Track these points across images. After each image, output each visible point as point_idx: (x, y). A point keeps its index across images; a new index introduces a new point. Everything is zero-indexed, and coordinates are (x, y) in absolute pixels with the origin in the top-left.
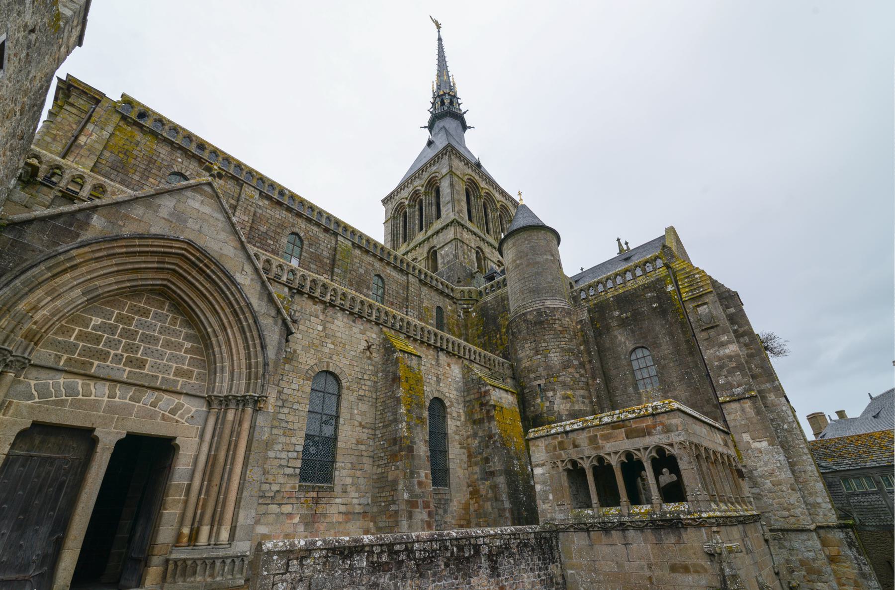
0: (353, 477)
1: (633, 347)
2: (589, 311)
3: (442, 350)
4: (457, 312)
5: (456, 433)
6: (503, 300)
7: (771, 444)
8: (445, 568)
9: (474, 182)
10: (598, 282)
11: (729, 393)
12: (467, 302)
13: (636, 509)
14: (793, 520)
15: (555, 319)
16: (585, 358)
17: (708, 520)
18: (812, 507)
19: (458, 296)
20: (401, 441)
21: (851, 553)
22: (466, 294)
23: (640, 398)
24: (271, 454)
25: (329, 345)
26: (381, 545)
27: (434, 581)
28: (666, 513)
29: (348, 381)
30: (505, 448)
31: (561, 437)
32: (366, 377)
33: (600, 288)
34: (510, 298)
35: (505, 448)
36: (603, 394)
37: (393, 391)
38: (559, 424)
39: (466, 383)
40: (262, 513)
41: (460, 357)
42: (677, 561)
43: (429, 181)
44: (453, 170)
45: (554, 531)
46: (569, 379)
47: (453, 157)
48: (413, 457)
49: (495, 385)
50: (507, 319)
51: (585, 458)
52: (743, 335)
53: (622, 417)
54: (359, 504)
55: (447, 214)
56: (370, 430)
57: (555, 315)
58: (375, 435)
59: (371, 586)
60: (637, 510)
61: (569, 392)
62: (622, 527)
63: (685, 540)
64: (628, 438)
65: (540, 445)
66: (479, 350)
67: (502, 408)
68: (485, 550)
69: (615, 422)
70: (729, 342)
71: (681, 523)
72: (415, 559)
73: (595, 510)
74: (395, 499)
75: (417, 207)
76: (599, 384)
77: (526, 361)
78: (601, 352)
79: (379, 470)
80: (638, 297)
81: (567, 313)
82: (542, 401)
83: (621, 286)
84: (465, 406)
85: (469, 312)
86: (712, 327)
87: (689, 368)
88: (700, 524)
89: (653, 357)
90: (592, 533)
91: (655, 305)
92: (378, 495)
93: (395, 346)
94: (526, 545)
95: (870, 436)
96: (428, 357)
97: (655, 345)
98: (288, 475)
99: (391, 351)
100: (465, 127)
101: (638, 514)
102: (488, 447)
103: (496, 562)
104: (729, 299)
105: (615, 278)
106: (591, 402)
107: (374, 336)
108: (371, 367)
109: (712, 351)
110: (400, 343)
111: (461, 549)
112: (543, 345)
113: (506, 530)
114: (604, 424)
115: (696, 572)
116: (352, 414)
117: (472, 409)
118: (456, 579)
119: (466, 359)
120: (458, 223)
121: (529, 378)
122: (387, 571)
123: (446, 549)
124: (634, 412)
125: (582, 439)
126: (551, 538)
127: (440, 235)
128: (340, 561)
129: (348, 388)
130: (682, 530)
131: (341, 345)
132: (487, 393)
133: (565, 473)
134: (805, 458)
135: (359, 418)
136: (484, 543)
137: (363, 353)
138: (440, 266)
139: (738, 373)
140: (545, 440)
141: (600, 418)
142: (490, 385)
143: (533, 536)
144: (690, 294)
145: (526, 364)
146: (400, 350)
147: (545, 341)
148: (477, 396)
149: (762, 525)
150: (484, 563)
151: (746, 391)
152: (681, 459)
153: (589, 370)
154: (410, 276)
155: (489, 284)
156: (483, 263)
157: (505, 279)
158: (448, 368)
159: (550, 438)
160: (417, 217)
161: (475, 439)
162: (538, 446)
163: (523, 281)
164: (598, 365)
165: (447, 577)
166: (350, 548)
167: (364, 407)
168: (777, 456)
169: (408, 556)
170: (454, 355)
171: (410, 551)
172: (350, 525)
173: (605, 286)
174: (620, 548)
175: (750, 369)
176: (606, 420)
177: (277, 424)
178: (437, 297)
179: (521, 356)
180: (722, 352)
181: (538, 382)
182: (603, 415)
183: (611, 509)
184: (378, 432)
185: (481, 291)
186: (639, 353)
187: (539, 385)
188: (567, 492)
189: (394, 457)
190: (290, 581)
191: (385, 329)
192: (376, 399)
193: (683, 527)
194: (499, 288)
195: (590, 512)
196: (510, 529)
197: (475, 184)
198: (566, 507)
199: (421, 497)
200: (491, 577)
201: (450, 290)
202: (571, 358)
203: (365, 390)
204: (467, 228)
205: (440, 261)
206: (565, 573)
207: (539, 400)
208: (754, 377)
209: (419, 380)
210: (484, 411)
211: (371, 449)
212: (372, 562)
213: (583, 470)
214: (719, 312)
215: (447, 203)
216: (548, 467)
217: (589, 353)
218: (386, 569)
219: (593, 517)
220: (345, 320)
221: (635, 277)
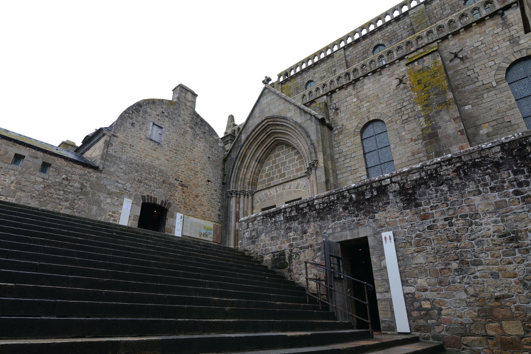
29: (390, 117)
59: (286, 229)
72: (315, 210)
118: (357, 216)
123: (344, 197)
129: (391, 121)
131: (375, 98)
135: (409, 136)
165: (347, 216)
169: (310, 209)
177: (345, 170)
203: (408, 114)
212: (286, 217)
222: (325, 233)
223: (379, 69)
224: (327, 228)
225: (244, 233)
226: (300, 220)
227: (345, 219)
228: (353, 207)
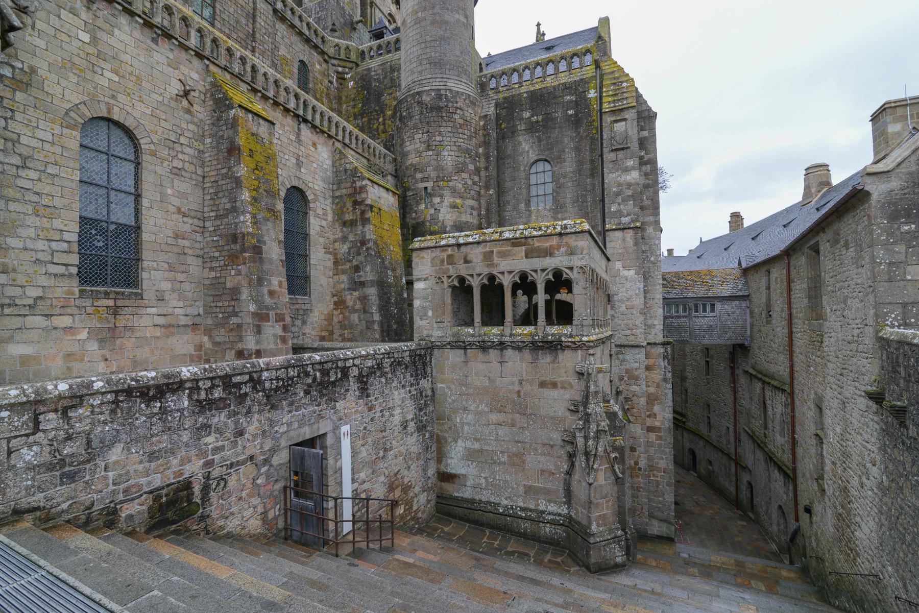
0: (173, 281)
1: (536, 158)
2: (497, 106)
3: (305, 121)
4: (328, 75)
6: (392, 70)
7: (637, 273)
8: (305, 396)
10: (514, 70)
11: (616, 221)
12: (344, 64)
13: (519, 330)
14: (632, 338)
15: (457, 108)
16: (482, 164)
17: (587, 344)
18: (649, 327)
19: (331, 51)
20: (244, 239)
21: (662, 363)
22: (342, 52)
23: (530, 216)
24: (13, 242)
25: (107, 74)
26: (212, 379)
27: (290, 412)
28: (548, 335)
29: (152, 142)
30: (380, 257)
32: (182, 140)
33: (515, 78)
34: (403, 67)
35: (380, 257)
36: (494, 207)
37: (230, 168)
38: (451, 235)
39: (336, 173)
40: (14, 327)
41: (330, 137)
42: (548, 378)
45: (429, 348)
46: (460, 186)
48: (261, 260)
49: (374, 180)
50: (395, 98)
51: (475, 276)
52: (646, 163)
53: (526, 233)
54: (186, 315)
56: (196, 221)
57: (457, 102)
58: (204, 227)
59: (198, 429)
60: (520, 331)
61: (458, 201)
62: (502, 346)
63: (560, 361)
64: (527, 257)
65: (426, 257)
66: (356, 131)
67: (380, 210)
68: (355, 372)
69: (516, 238)
70: (633, 168)
71: (561, 345)
72: (264, 390)
73: (477, 329)
74: (237, 310)
76: (491, 195)
77: (413, 156)
78: (500, 158)
79: (213, 274)
80: (555, 97)
82: (426, 207)
83: (539, 80)
84: (333, 203)
85: (344, 79)
86: (623, 149)
87: (586, 190)
88: (578, 346)
89: (553, 173)
90: (469, 351)
91: (570, 112)
92: (212, 304)
93: (231, 98)
94: (399, 364)
95: (699, 273)
96: (285, 127)
97: (560, 160)
98: (55, 275)
99: (225, 105)
101: (520, 335)
102: (360, 254)
103: (366, 383)
104: (647, 118)
105: (535, 68)
106: (479, 215)
107: (195, 76)
108: (192, 127)
109: (614, 175)
110: (239, 95)
111: (325, 373)
112: (438, 138)
113: (379, 350)
114: (504, 240)
115: (563, 387)
116: (163, 194)
117: (342, 208)
119: (338, 141)
121: (414, 178)
122: (223, 408)
123: (307, 374)
124: (540, 229)
125: (476, 254)
126: (425, 355)
128: (143, 406)
130: (560, 352)
131: (134, 79)
132: (363, 188)
133: (450, 290)
134: (658, 287)
135: (176, 202)
136: (354, 365)
137: (176, 101)
139: (631, 202)
141: (501, 233)
142: (369, 179)
143: (408, 353)
144: (612, 105)
145: (412, 159)
146: (240, 106)
148: (350, 191)
149: (611, 343)
150: (353, 385)
151: (633, 221)
152: (577, 283)
153: (483, 179)
155: (375, 43)
156: (369, 11)
157: (398, 41)
158: (313, 149)
159: (438, 250)
162: (423, 258)
163: (423, 45)
164: (494, 173)
166: (158, 387)
167: (184, 186)
168: (638, 283)
169: (254, 388)
170: (323, 132)
171: (256, 382)
172: (173, 340)
173: (520, 76)
174: (495, 365)
175: (642, 200)
176: (507, 235)
177: (18, 195)
178: (301, 46)
179: (408, 149)
180: (623, 178)
181: (425, 185)
182: (504, 229)
183: (493, 329)
184: (208, 224)
185: (363, 52)
186: (540, 166)
187: (426, 188)
188: (449, 308)
189: (233, 258)
190: (45, 442)
191: (212, 68)
192: (204, 177)
193: (561, 349)
194: (389, 52)
195: (470, 330)
196: (384, 347)
198: (445, 325)
199: (273, 309)
200: (359, 399)
201: (320, 40)
202: (467, 161)
203: (183, 161)
206: (434, 386)
207: (422, 206)
208: (642, 208)
209: (270, 158)
210: (358, 212)
211: (198, 245)
212: (198, 401)
214: (633, 133)
216: (432, 281)
217: (487, 157)
218: (222, 406)
219: (473, 336)
220: (137, 34)
221: (557, 72)
222: (277, 432)
223: (160, 32)
224: (280, 423)
225: (10, 453)
226: (232, 408)
227: (305, 409)
228: (316, 391)
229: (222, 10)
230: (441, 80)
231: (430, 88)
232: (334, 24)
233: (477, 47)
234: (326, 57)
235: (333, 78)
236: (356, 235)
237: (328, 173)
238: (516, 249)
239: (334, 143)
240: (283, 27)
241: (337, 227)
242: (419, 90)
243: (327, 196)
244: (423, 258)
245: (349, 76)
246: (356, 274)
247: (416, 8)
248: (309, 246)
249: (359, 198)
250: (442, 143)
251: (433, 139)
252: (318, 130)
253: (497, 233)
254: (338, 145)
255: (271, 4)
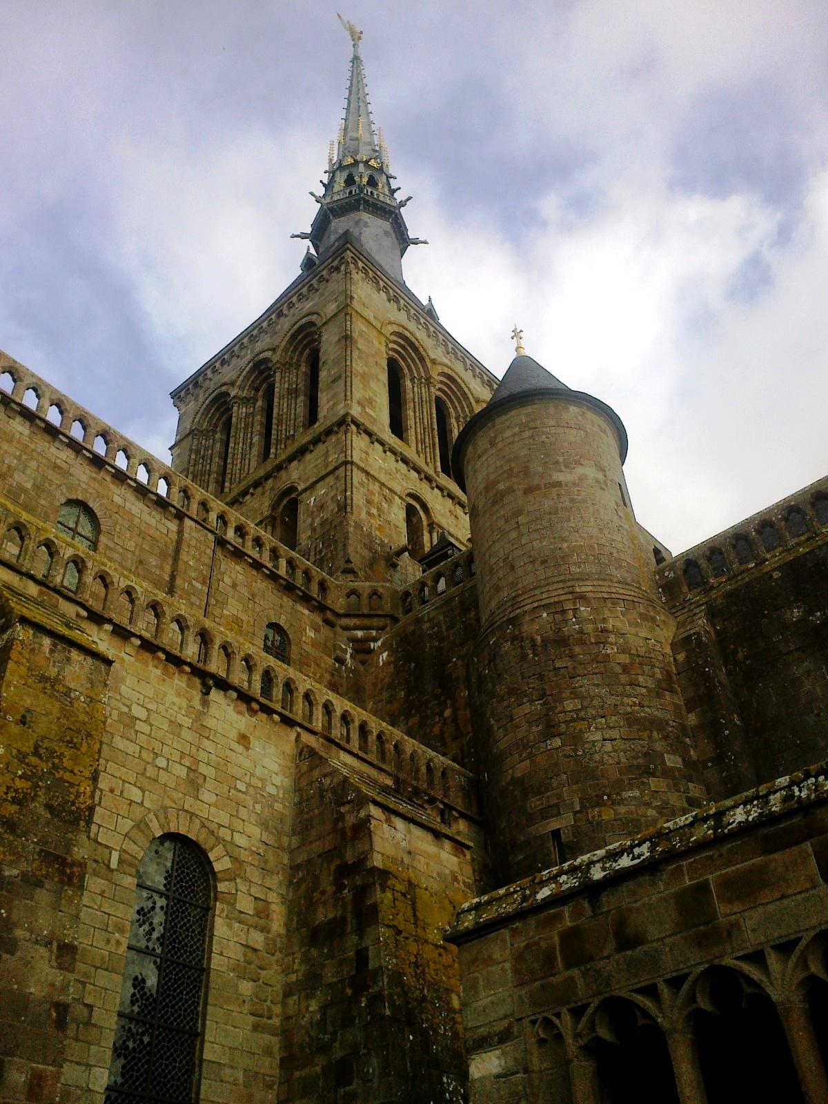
2: (713, 614)
3: (223, 685)
4: (335, 647)
5: (248, 968)
9: (412, 344)
12: (366, 622)
19: (338, 602)
31: (576, 914)
43: (294, 337)
44: (356, 305)
47: (357, 276)
55: (332, 408)
57: (604, 620)
65: (497, 956)
75: (259, 403)
81: (644, 617)
84: (290, 883)
85: (370, 651)
100: (403, 240)
114: (734, 835)
120: (354, 422)
127: (308, 457)
132: (362, 829)
138: (304, 537)
140: (515, 932)
141: (720, 814)
142: (376, 803)
147: (575, 694)
154: (188, 522)
158: (240, 748)
159: (532, 921)
160: (257, 428)
161: (308, 997)
162: (489, 961)
187: (556, 834)
197: (416, 350)
202: (659, 746)
204: (382, 443)
205: (303, 521)
213: (656, 1038)
215: (334, 381)
229: (111, 545)
230: (561, 585)
231: (536, 604)
232: (349, 561)
233: (640, 519)
234: (329, 615)
235: (345, 651)
236: (341, 962)
237: (278, 806)
238: (775, 856)
239: (298, 735)
240: (238, 568)
241: (296, 948)
242: (512, 615)
243: (271, 865)
244: (489, 961)
245: (379, 643)
246: (342, 1091)
247: (492, 477)
248: (206, 1004)
249: (350, 856)
250: (582, 714)
251: (559, 709)
252: (255, 706)
253: (705, 820)
254: (307, 738)
255: (211, 532)
